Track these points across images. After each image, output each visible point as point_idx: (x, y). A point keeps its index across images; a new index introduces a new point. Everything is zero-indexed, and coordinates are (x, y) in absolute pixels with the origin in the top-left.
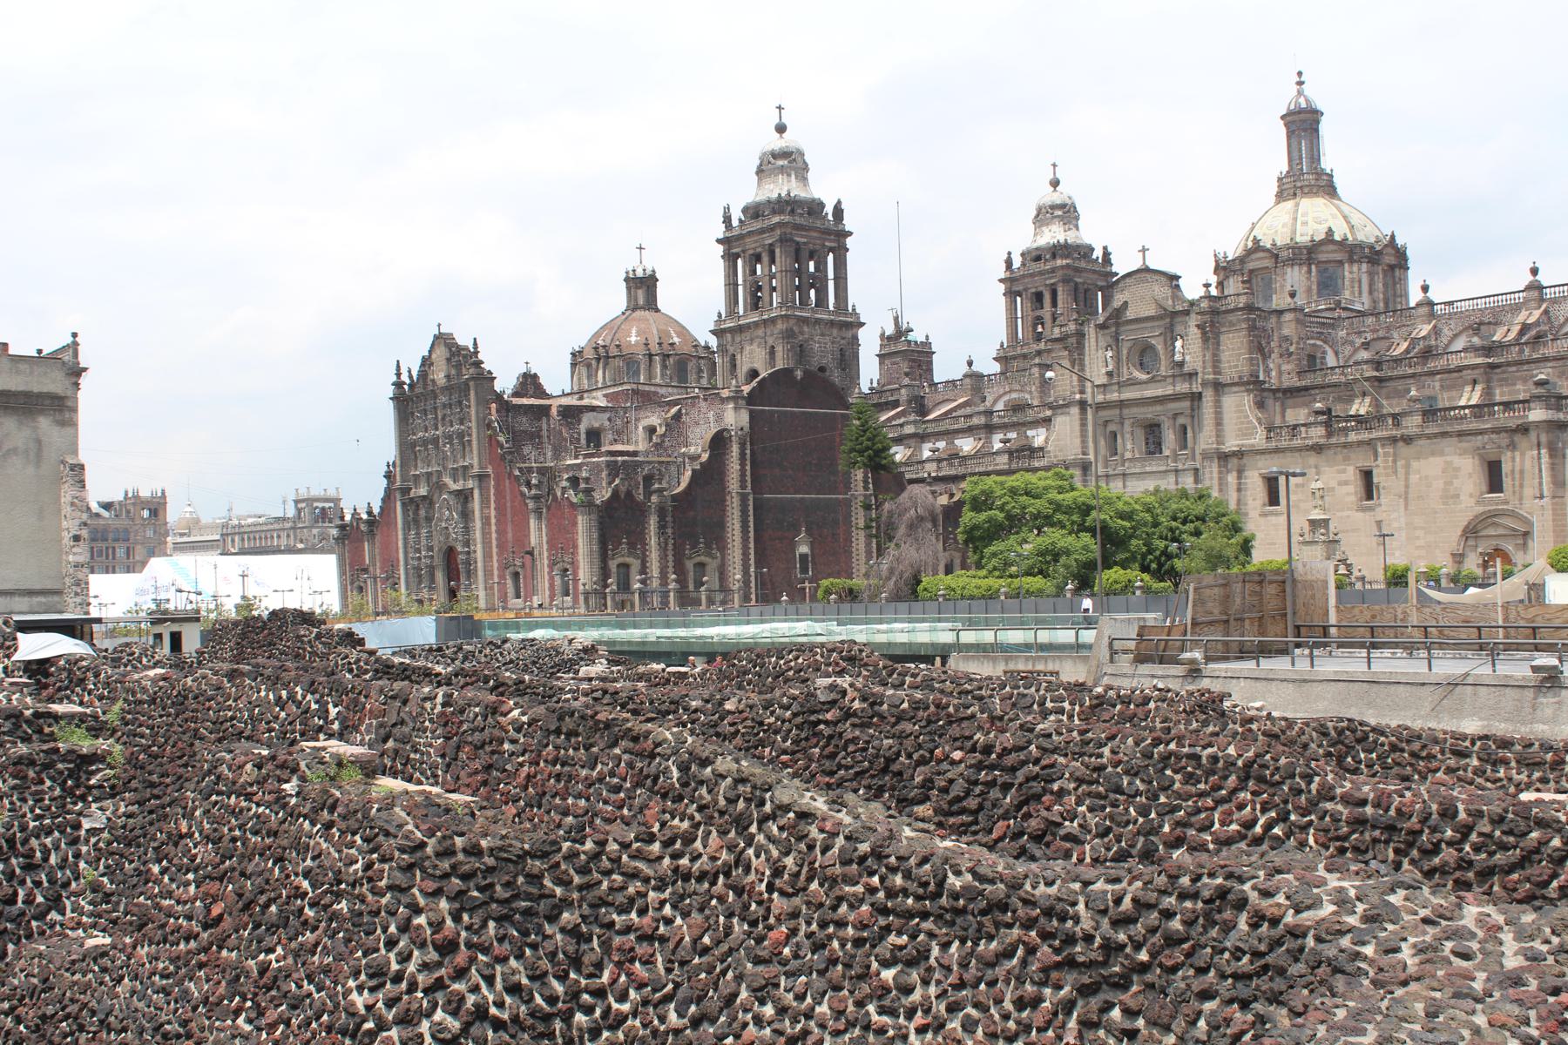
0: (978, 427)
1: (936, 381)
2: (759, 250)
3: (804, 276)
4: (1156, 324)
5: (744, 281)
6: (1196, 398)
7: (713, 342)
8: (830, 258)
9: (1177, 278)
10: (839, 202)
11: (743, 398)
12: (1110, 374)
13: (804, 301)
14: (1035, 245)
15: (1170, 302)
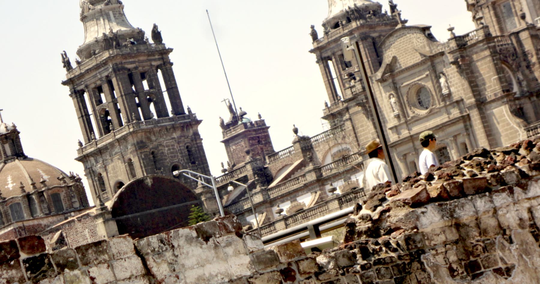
0: (311, 184)
1: (276, 150)
2: (99, 83)
3: (141, 94)
4: (421, 68)
5: (94, 110)
6: (466, 119)
7: (79, 170)
8: (160, 74)
9: (428, 28)
10: (155, 27)
11: (109, 212)
12: (398, 117)
13: (148, 116)
14: (332, 15)
15: (427, 49)
